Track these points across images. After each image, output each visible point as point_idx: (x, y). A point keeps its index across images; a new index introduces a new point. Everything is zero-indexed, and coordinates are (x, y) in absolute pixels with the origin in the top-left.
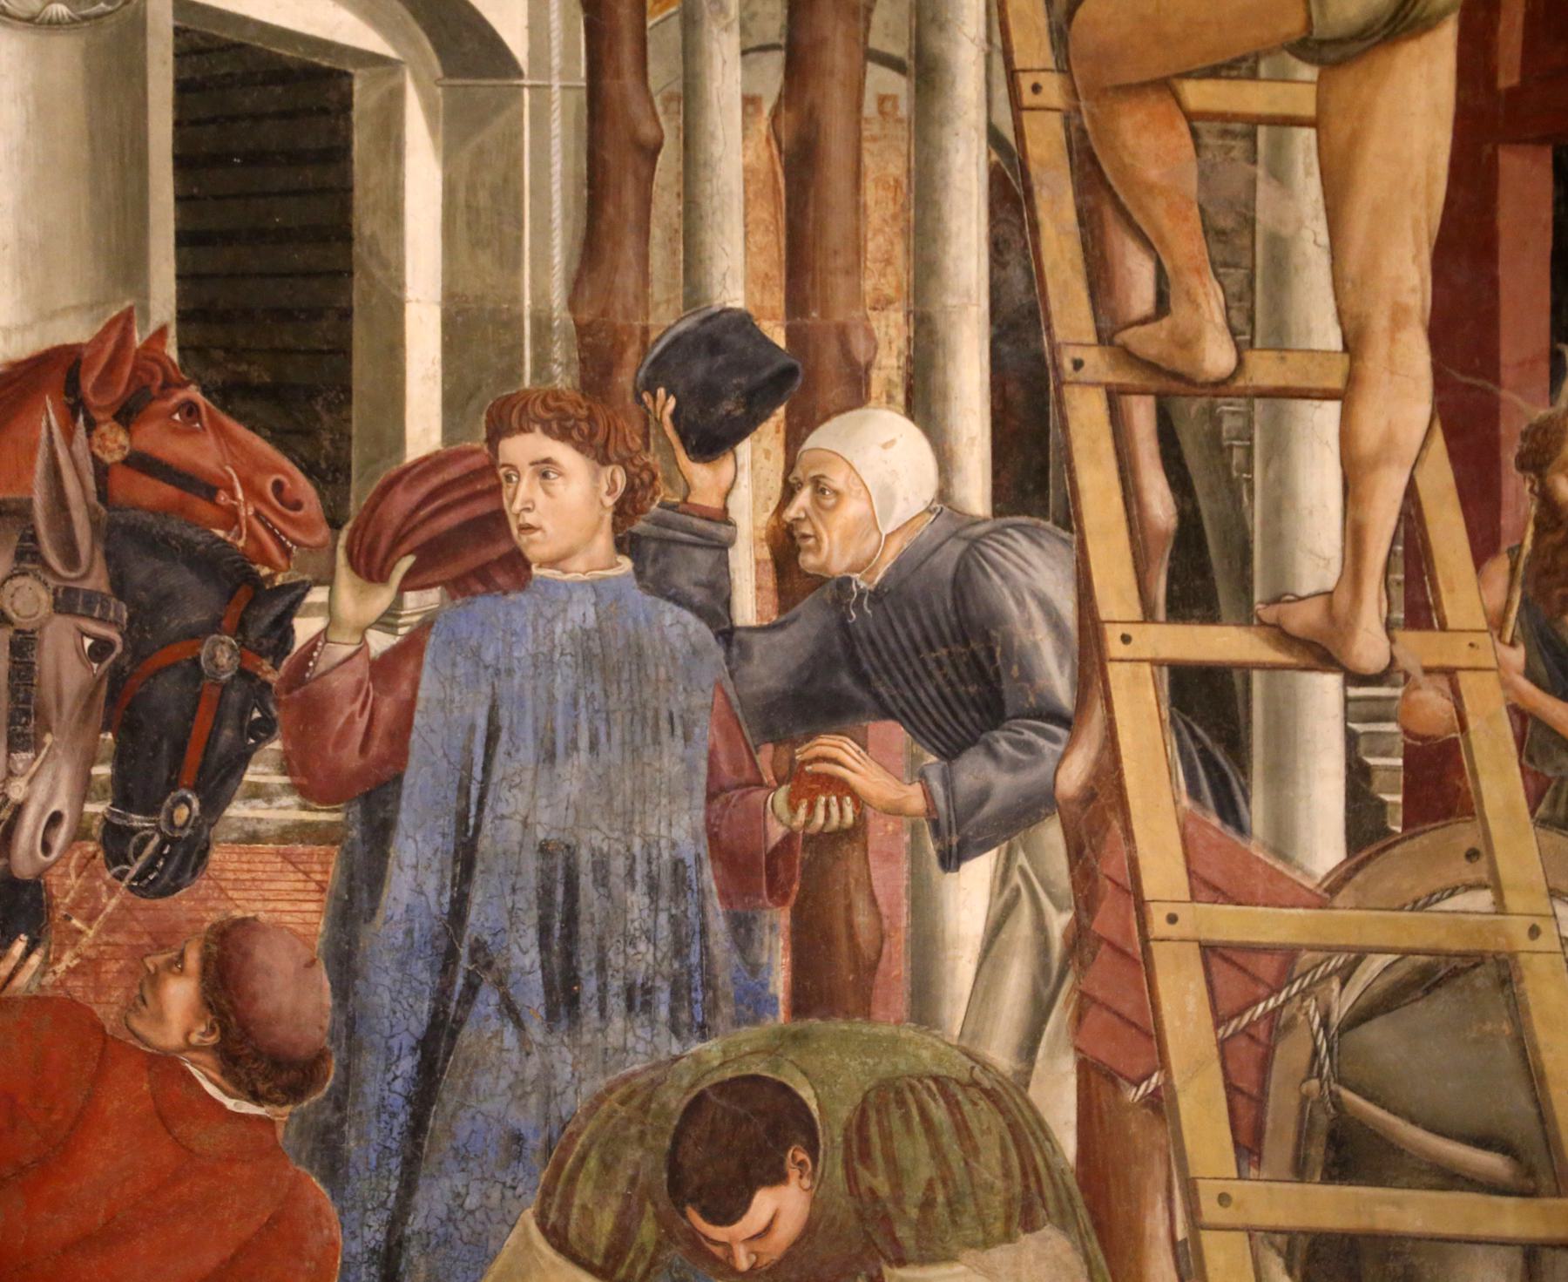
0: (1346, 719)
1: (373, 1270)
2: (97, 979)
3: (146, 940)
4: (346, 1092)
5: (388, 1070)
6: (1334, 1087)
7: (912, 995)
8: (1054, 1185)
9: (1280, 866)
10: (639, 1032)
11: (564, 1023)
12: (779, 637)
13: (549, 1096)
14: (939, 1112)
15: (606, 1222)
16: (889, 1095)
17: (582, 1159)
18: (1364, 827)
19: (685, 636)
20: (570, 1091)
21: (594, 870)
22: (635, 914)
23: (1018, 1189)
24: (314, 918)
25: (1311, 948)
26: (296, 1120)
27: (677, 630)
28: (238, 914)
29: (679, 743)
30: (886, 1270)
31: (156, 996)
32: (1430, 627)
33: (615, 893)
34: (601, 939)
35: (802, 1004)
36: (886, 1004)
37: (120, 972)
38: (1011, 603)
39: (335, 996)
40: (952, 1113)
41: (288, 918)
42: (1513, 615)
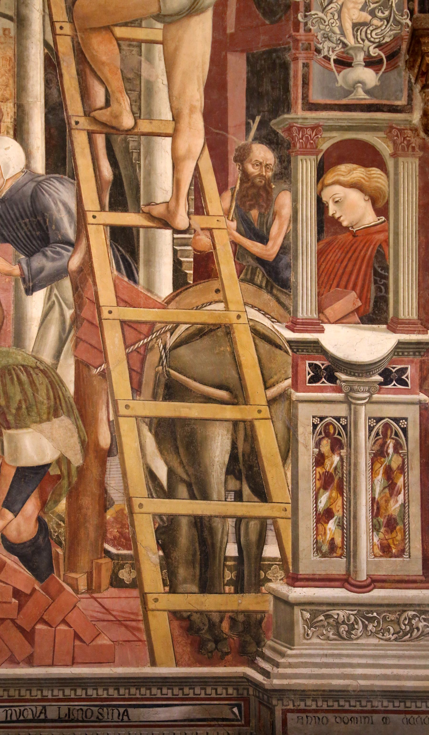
0: (173, 245)
6: (167, 369)
7: (15, 337)
8: (66, 402)
9: (149, 294)
14: (24, 377)
18: (179, 281)
23: (52, 403)
25: (160, 322)
32: (203, 214)
36: (5, 341)
38: (52, 204)
40: (29, 378)
42: (232, 211)
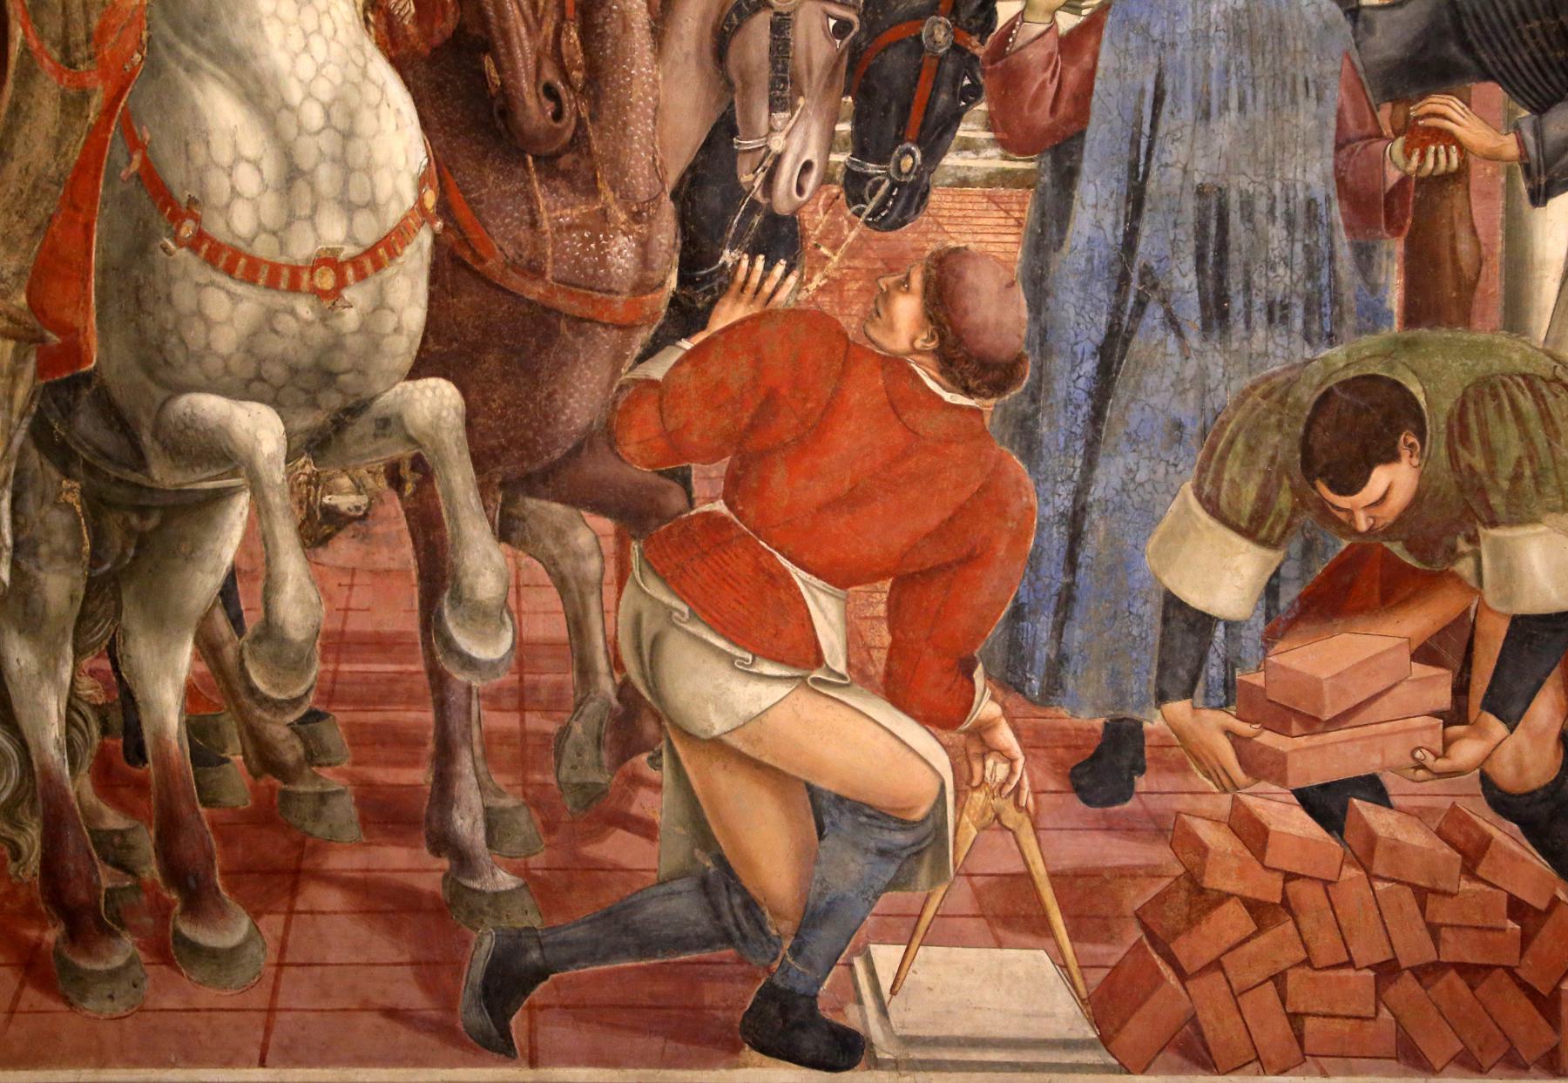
1: (1063, 529)
2: (841, 296)
3: (879, 265)
4: (1040, 388)
5: (1073, 370)
7: (1505, 308)
10: (1278, 340)
11: (1216, 334)
12: (1398, 13)
13: (1204, 392)
14: (1527, 404)
15: (1250, 493)
16: (1485, 389)
17: (1231, 442)
19: (1319, 14)
20: (1222, 388)
21: (1242, 209)
22: (1275, 244)
24: (1013, 248)
26: (1000, 411)
27: (1312, 9)
28: (952, 244)
29: (1313, 103)
30: (1482, 530)
31: (887, 309)
33: (1259, 227)
34: (1247, 264)
35: (1413, 316)
36: (1483, 315)
37: (859, 290)
39: (1030, 311)
40: (1538, 404)
41: (991, 248)
